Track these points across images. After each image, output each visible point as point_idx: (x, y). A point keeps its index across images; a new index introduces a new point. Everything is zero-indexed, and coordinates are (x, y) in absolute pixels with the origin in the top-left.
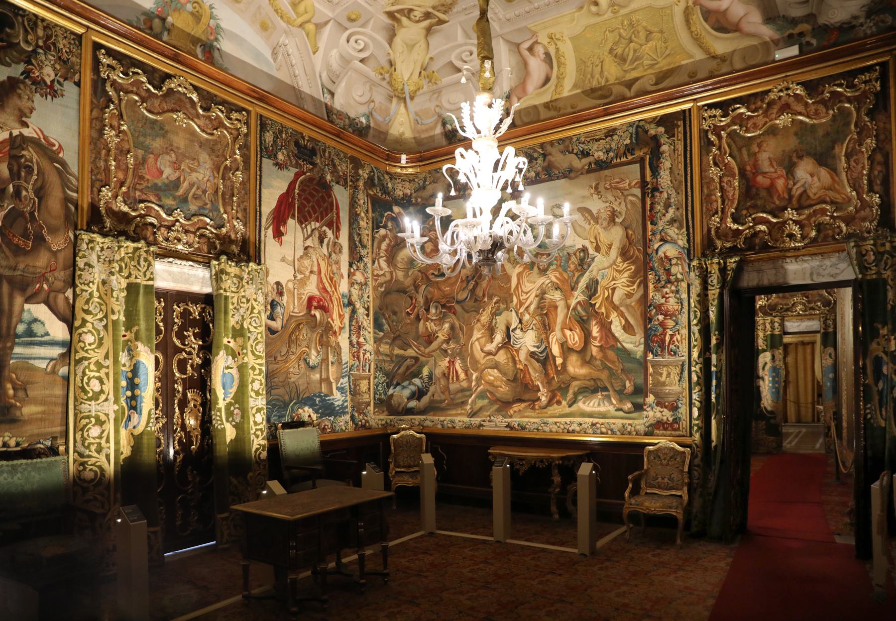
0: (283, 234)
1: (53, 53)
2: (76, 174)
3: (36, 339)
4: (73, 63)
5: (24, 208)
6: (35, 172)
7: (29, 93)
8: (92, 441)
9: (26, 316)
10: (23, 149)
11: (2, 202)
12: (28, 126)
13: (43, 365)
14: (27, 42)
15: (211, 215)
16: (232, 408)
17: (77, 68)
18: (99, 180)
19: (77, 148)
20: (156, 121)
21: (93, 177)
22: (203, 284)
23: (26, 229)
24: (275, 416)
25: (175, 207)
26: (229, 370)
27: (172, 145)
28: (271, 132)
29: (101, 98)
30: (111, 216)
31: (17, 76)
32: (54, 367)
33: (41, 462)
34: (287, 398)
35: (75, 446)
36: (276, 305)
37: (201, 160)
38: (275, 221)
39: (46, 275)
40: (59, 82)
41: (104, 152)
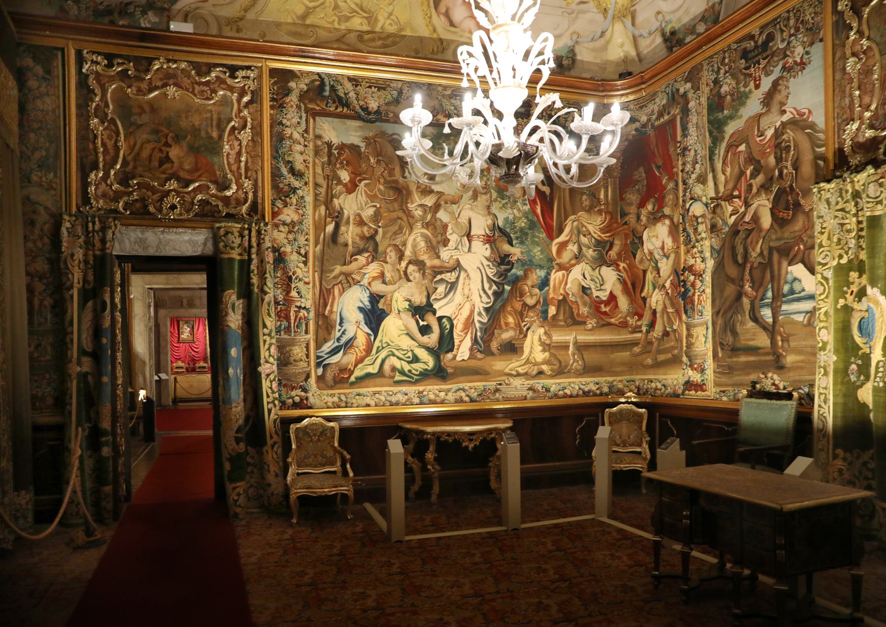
6: (792, 148)
7: (785, 83)
9: (790, 278)
13: (800, 318)
23: (788, 201)
30: (858, 150)
40: (807, 53)
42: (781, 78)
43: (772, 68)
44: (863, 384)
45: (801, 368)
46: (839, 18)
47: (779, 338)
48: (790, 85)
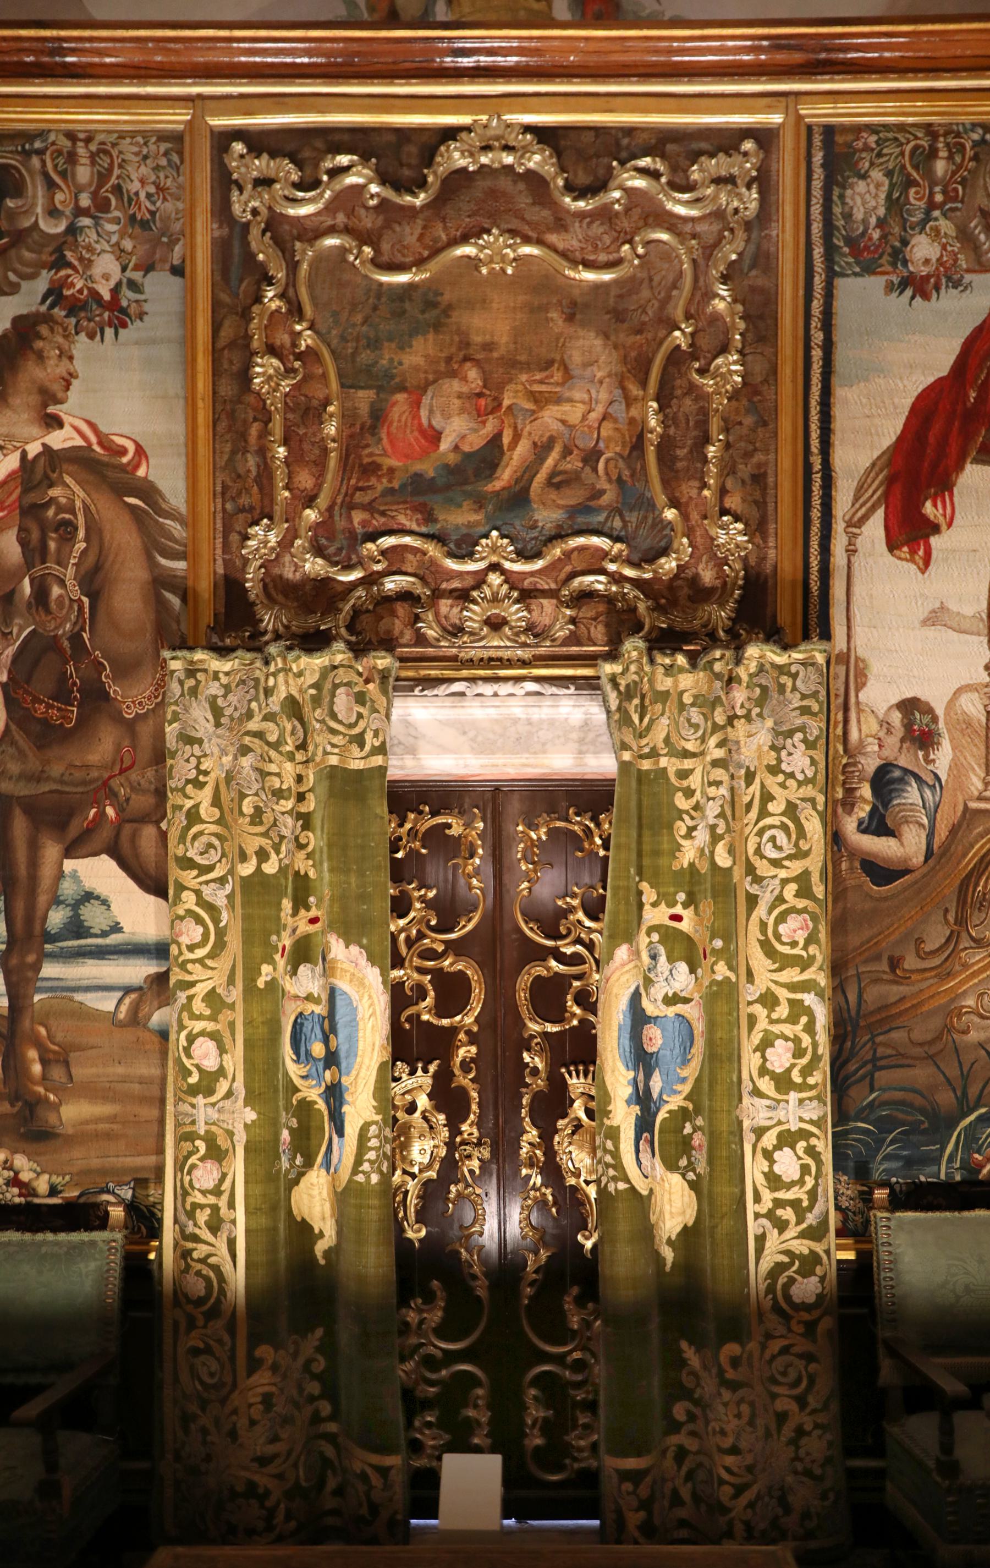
0: (936, 529)
1: (117, 214)
2: (183, 509)
3: (90, 941)
4: (166, 219)
5: (57, 628)
6: (81, 534)
7: (60, 339)
8: (199, 1198)
9: (68, 889)
10: (51, 485)
11: (7, 626)
12: (60, 425)
13: (106, 1003)
14: (53, 212)
15: (617, 523)
16: (688, 1129)
17: (177, 227)
18: (242, 510)
19: (182, 439)
20: (411, 286)
21: (229, 506)
22: (584, 746)
23: (63, 677)
24: (887, 1158)
25: (482, 530)
26: (680, 1008)
27: (468, 344)
28: (877, 175)
29: (241, 281)
30: (280, 598)
31: (34, 309)
32: (135, 1009)
34: (946, 1099)
36: (901, 780)
37: (576, 357)
38: (898, 489)
39: (112, 782)
40: (134, 286)
41: (254, 430)
42: (47, 319)
43: (12, 277)
44: (301, 1174)
45: (108, 1136)
46: (230, 236)
47: (33, 1054)
48: (75, 353)
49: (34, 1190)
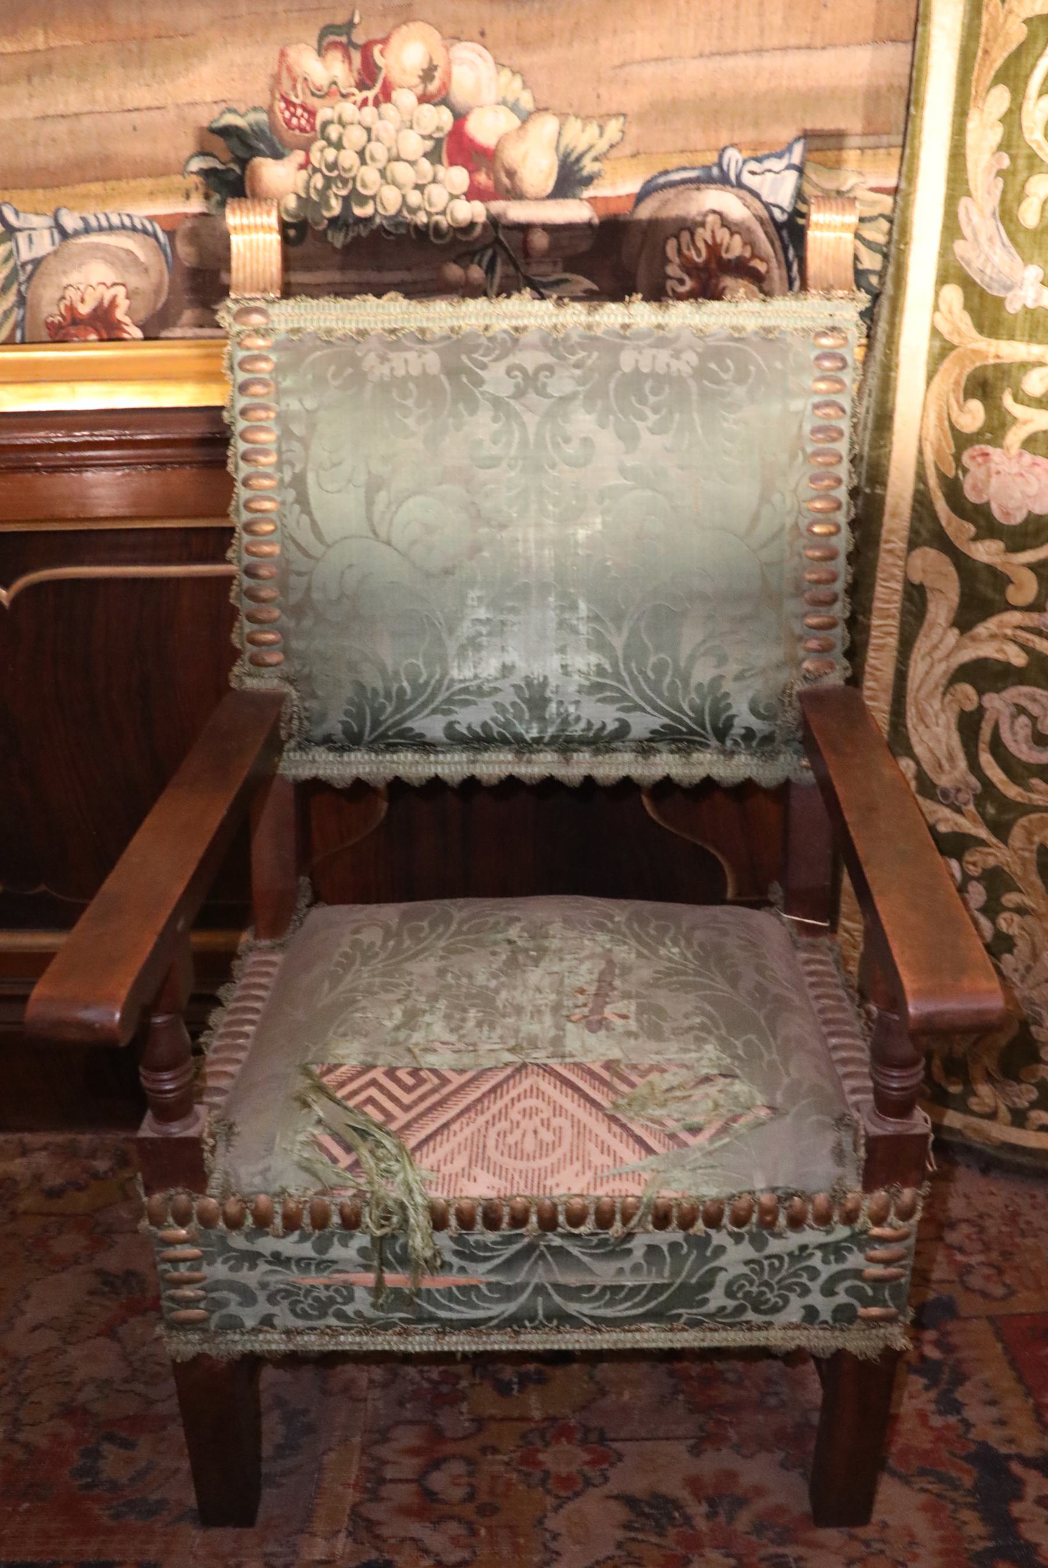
33: (660, 338)
35: (951, 229)
49: (511, 174)
